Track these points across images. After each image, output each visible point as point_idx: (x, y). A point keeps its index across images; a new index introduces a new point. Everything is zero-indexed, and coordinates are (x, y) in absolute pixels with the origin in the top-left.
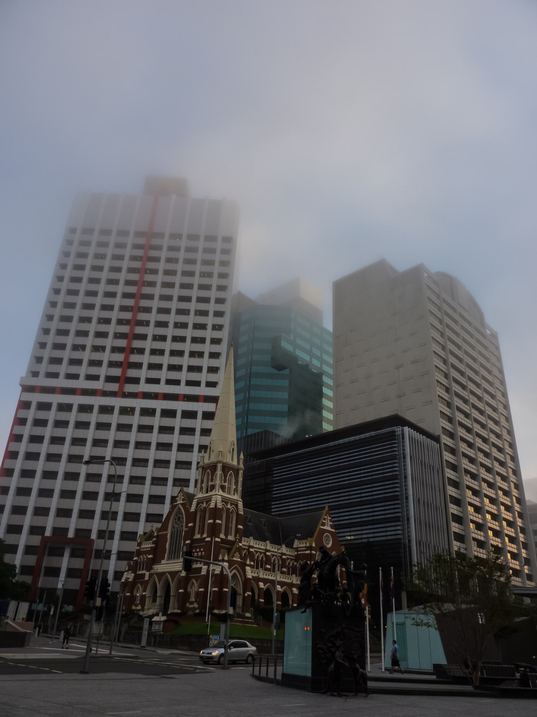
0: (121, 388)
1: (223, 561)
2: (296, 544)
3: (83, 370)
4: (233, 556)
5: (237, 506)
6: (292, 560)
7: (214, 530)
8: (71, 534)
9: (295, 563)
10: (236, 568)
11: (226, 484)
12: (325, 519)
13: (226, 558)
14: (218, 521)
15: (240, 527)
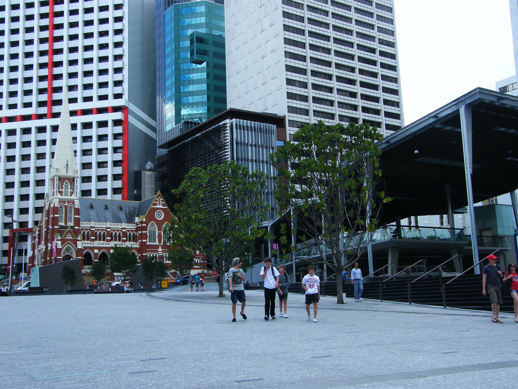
0: (50, 110)
1: (57, 240)
2: (137, 220)
3: (18, 100)
4: (66, 236)
5: (73, 203)
6: (132, 231)
7: (55, 221)
8: (30, 226)
9: (136, 233)
10: (69, 243)
11: (63, 190)
12: (156, 201)
13: (59, 238)
14: (56, 216)
15: (76, 216)
